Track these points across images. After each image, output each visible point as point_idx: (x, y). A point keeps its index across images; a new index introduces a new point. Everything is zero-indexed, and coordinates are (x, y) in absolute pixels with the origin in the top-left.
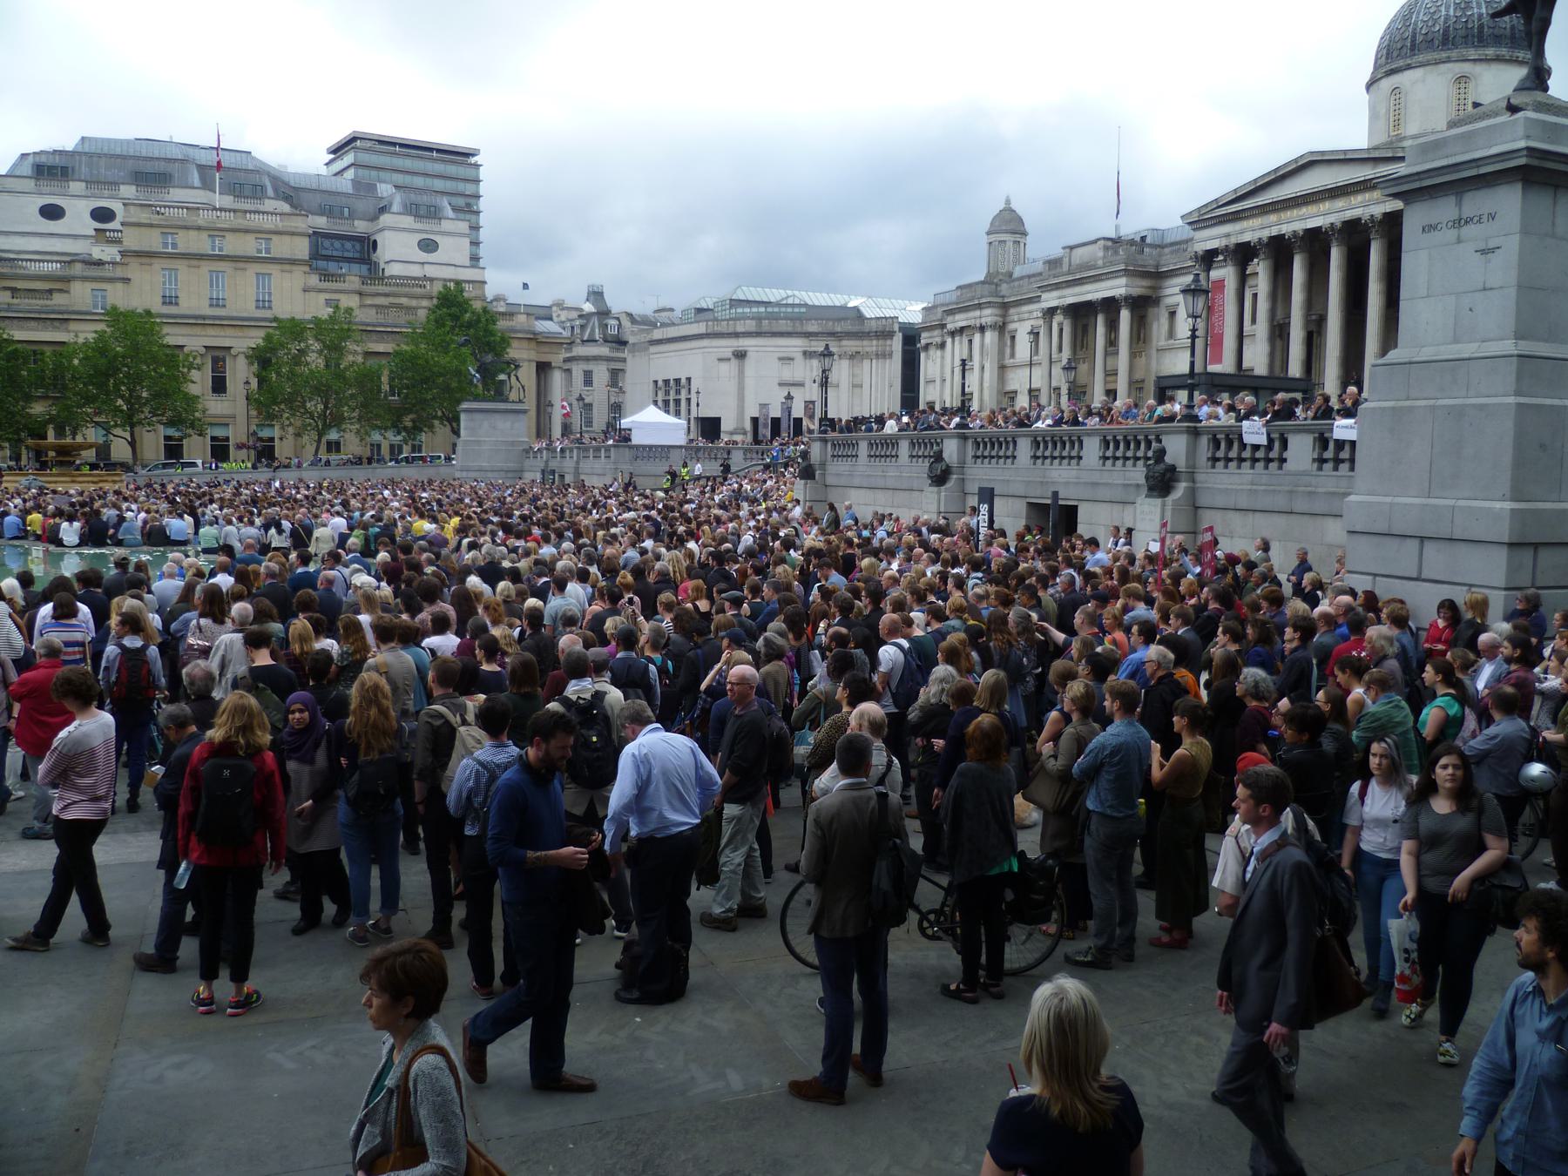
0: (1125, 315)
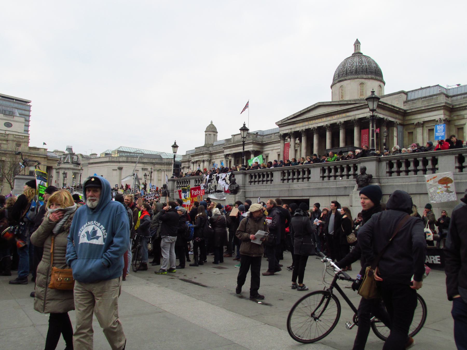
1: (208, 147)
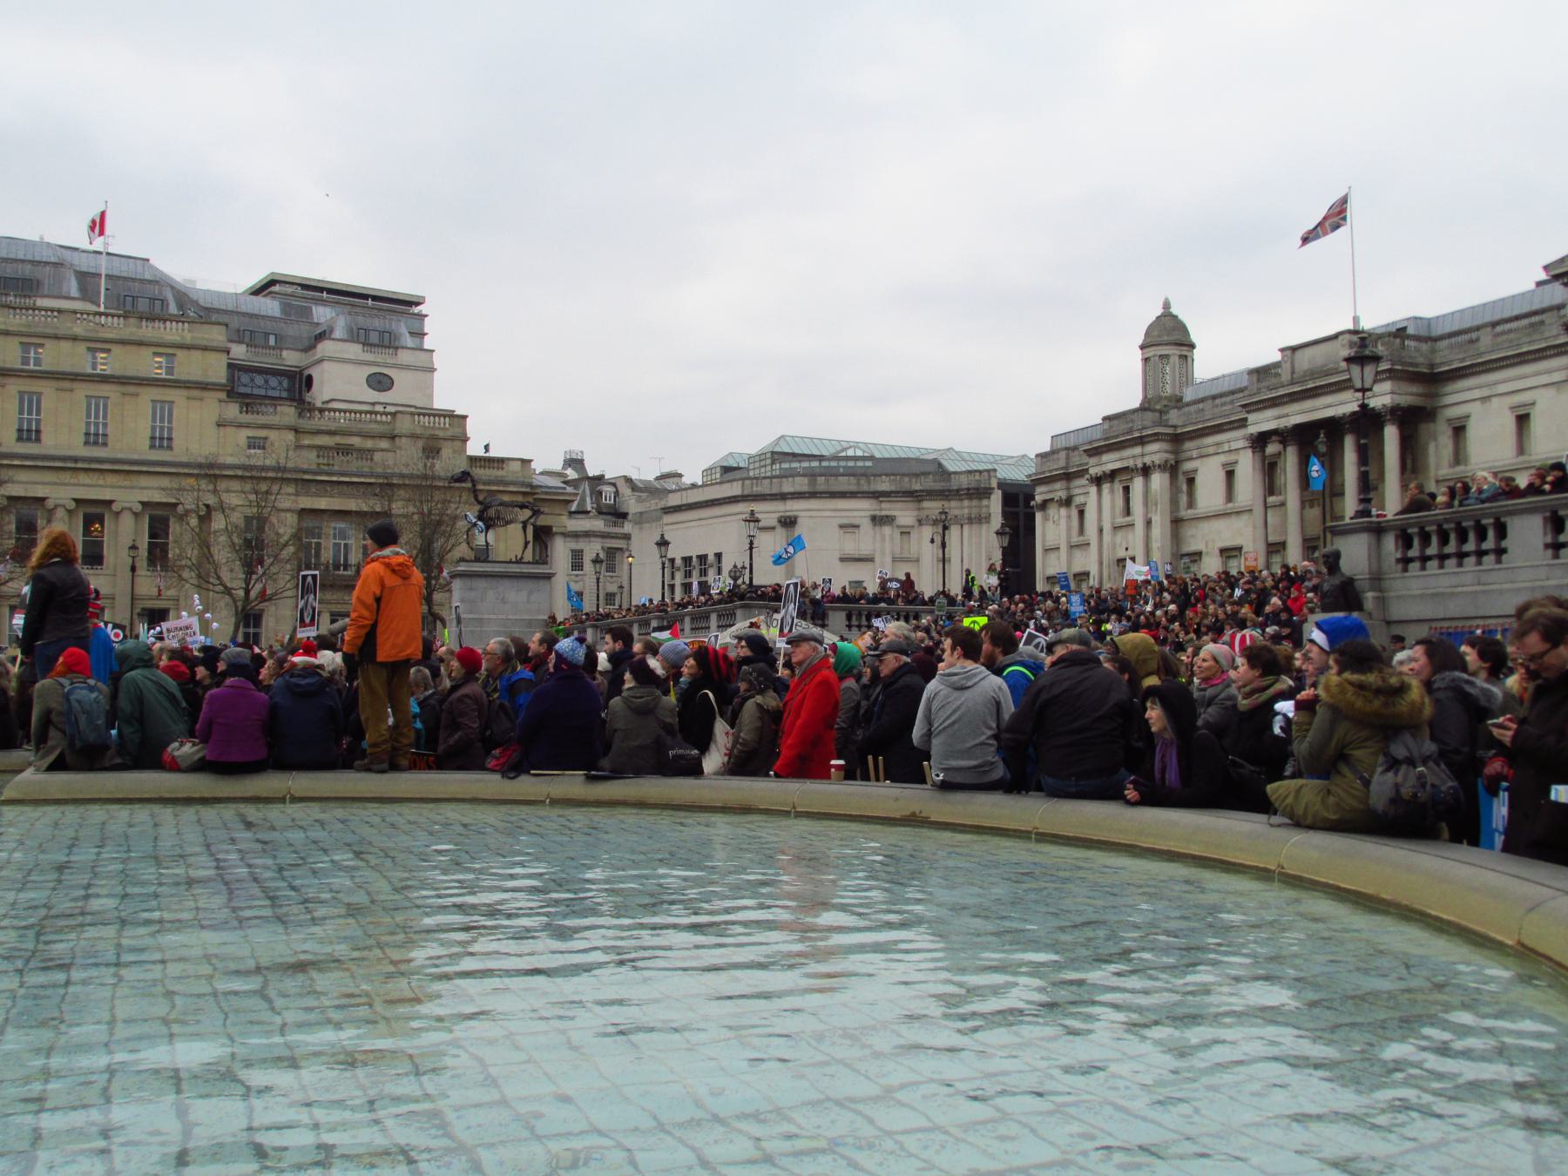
0: (1391, 434)
1: (1161, 412)
